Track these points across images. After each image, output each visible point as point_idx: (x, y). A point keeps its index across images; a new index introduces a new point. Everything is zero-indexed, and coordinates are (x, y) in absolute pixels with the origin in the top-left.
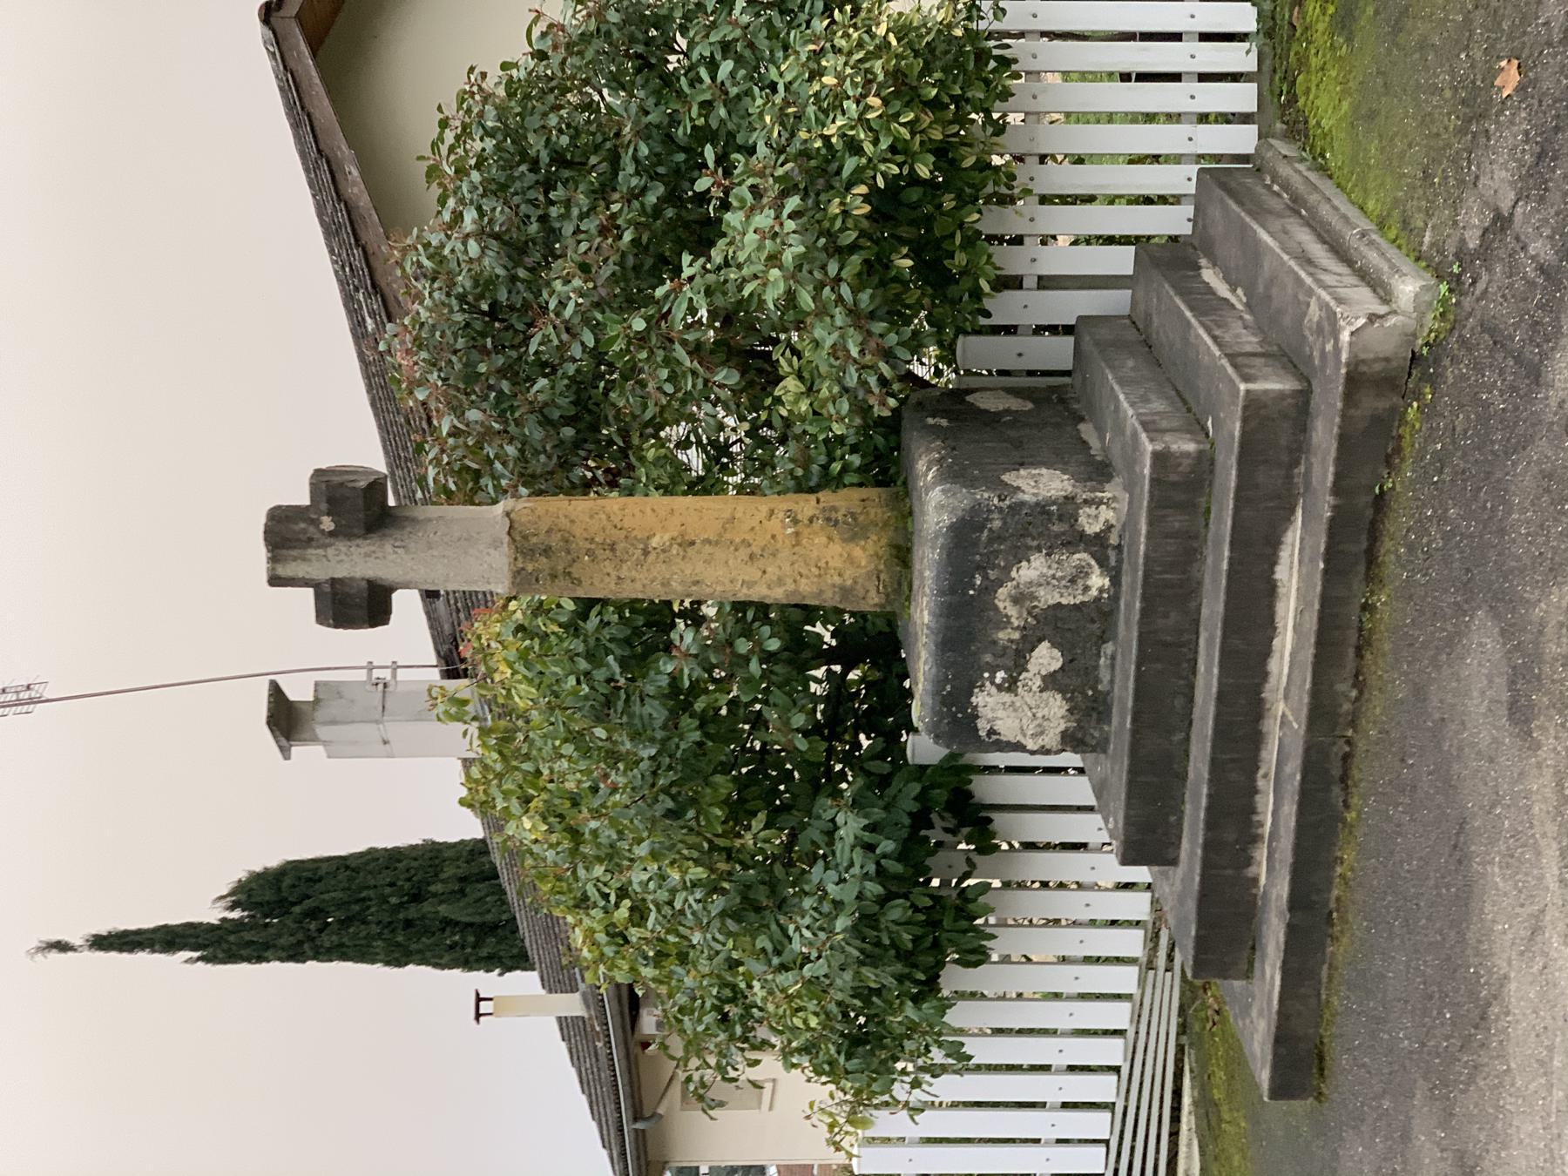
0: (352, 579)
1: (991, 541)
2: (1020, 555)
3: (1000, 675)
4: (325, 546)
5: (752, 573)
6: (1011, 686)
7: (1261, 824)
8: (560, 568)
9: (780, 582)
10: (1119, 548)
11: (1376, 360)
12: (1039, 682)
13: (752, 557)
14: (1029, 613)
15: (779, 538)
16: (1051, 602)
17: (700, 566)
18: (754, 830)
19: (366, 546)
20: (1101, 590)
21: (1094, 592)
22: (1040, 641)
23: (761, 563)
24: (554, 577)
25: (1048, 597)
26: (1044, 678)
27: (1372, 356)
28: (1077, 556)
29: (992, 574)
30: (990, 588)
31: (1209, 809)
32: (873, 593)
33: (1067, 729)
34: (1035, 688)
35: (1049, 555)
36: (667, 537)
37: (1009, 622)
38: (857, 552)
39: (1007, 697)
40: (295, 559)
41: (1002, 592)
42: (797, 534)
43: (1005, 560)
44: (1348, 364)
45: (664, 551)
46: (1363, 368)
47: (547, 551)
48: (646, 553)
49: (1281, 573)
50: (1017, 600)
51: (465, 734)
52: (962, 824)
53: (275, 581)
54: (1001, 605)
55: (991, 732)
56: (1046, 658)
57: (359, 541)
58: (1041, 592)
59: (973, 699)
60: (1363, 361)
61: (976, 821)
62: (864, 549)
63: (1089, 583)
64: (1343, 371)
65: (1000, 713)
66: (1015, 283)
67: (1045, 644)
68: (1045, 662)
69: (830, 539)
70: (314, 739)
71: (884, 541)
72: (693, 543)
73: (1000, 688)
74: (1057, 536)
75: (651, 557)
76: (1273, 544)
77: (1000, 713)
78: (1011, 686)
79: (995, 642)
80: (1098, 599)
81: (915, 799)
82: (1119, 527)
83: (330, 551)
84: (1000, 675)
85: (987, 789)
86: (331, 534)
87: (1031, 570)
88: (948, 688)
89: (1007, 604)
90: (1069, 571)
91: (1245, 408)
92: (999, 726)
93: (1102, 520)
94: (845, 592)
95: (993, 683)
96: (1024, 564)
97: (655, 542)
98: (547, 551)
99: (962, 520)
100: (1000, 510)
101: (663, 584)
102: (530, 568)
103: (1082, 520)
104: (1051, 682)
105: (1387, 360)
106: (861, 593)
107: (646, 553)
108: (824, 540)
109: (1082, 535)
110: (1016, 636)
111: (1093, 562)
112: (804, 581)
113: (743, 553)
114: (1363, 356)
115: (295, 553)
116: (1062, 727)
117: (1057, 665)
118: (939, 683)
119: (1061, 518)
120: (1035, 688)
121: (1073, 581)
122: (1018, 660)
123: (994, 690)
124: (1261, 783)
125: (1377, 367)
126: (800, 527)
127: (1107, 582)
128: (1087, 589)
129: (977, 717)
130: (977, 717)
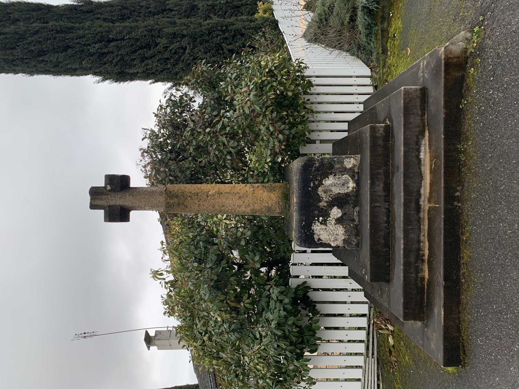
0: (115, 206)
1: (315, 171)
2: (326, 176)
3: (321, 218)
4: (107, 195)
5: (240, 202)
6: (324, 223)
7: (424, 255)
9: (249, 206)
10: (358, 173)
11: (454, 57)
12: (334, 221)
13: (240, 197)
14: (329, 197)
16: (337, 192)
17: (224, 200)
18: (243, 300)
19: (120, 195)
20: (353, 188)
21: (351, 189)
22: (334, 206)
23: (243, 199)
24: (179, 204)
25: (336, 190)
26: (336, 220)
27: (453, 56)
28: (344, 176)
29: (317, 183)
30: (316, 187)
31: (404, 249)
32: (277, 209)
33: (345, 239)
34: (333, 223)
35: (335, 175)
36: (214, 191)
37: (323, 199)
38: (272, 195)
39: (323, 227)
40: (98, 199)
41: (320, 189)
42: (254, 190)
43: (320, 177)
44: (445, 59)
45: (213, 196)
46: (450, 61)
47: (177, 197)
48: (207, 196)
49: (422, 156)
50: (325, 192)
51: (160, 283)
52: (307, 307)
53: (93, 207)
54: (320, 194)
55: (319, 239)
56: (336, 212)
57: (119, 193)
58: (333, 189)
59: (312, 227)
60: (450, 58)
61: (311, 305)
62: (274, 194)
63: (349, 185)
64: (443, 62)
65: (322, 232)
66: (314, 142)
67: (336, 207)
68: (335, 214)
69: (264, 191)
70: (155, 345)
71: (280, 192)
72: (222, 193)
73: (321, 223)
74: (337, 169)
75: (209, 198)
76: (418, 144)
77: (322, 232)
78: (324, 223)
79: (319, 207)
80: (353, 191)
81: (294, 293)
82: (358, 165)
83: (109, 197)
84: (321, 218)
85: (315, 296)
86: (110, 191)
87: (329, 181)
88: (304, 223)
89: (322, 193)
91: (404, 94)
92: (322, 237)
93: (352, 163)
94: (269, 209)
95: (319, 222)
96: (327, 179)
97: (210, 193)
98: (177, 197)
99: (305, 164)
100: (318, 161)
101: (213, 207)
102: (172, 202)
103: (345, 163)
104: (339, 221)
105: (458, 57)
106: (274, 209)
107: (207, 196)
108: (262, 192)
109: (346, 168)
110: (325, 204)
111: (350, 178)
112: (256, 205)
113: (237, 196)
114: (450, 56)
115: (98, 197)
116: (343, 238)
117: (340, 215)
118: (300, 221)
119: (338, 163)
120: (333, 223)
121: (343, 185)
122: (326, 214)
123: (319, 224)
124: (422, 238)
125: (455, 60)
126: (254, 189)
127: (355, 185)
128: (348, 187)
129: (314, 234)
130: (314, 234)
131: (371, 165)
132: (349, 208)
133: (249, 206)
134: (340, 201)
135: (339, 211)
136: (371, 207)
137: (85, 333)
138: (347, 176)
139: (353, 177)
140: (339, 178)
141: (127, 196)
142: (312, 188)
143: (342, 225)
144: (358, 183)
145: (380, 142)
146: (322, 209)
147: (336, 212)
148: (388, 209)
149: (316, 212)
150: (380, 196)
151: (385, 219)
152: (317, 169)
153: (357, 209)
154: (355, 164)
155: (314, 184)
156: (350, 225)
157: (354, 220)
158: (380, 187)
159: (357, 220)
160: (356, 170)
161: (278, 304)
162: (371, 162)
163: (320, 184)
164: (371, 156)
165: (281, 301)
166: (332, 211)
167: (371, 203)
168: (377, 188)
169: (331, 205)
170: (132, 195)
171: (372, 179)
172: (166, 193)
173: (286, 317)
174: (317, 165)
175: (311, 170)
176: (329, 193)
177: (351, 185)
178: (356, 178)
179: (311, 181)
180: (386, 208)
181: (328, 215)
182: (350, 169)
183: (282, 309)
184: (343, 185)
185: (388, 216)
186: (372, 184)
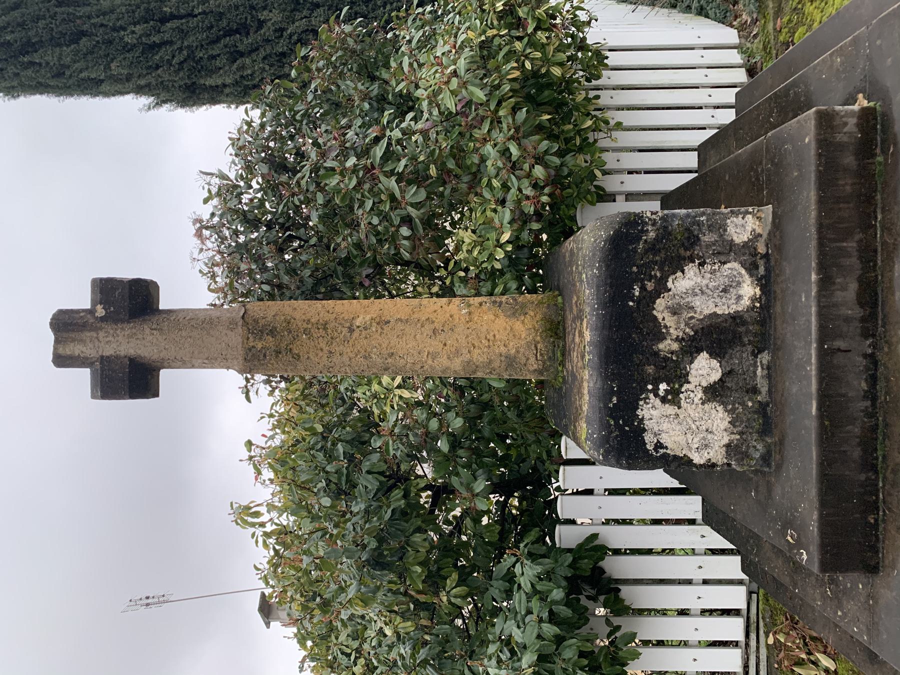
0: (117, 357)
1: (646, 251)
2: (677, 265)
3: (663, 387)
4: (97, 329)
5: (435, 345)
6: (673, 398)
8: (283, 345)
9: (457, 352)
10: (766, 256)
12: (700, 394)
13: (434, 331)
14: (687, 324)
15: (456, 317)
16: (707, 312)
18: (447, 589)
19: (128, 329)
20: (753, 299)
21: (746, 302)
22: (699, 351)
24: (278, 352)
25: (705, 307)
26: (706, 390)
28: (728, 265)
29: (650, 286)
30: (649, 299)
32: (532, 360)
33: (731, 441)
34: (696, 400)
35: (702, 264)
36: (368, 317)
37: (668, 333)
38: (518, 326)
39: (670, 409)
40: (73, 340)
41: (660, 303)
42: (470, 313)
43: (661, 269)
45: (365, 329)
47: (273, 332)
48: (351, 330)
51: (253, 535)
52: (599, 593)
53: (61, 360)
54: (660, 317)
55: (659, 446)
56: (705, 369)
57: (125, 325)
58: (697, 302)
59: (639, 412)
61: (609, 590)
62: (523, 322)
63: (741, 292)
67: (704, 355)
68: (704, 372)
69: (496, 316)
70: (278, 619)
71: (539, 317)
72: (389, 322)
73: (664, 400)
74: (708, 246)
75: (356, 334)
77: (665, 426)
78: (673, 398)
79: (656, 354)
80: (752, 308)
81: (569, 566)
82: (765, 236)
83: (101, 334)
84: (663, 387)
85: (618, 567)
86: (102, 319)
87: (686, 281)
88: (615, 400)
89: (666, 315)
90: (721, 281)
92: (665, 439)
93: (749, 229)
94: (511, 361)
95: (656, 395)
96: (679, 274)
97: (358, 322)
98: (273, 332)
99: (618, 233)
100: (654, 223)
101: (365, 357)
102: (259, 346)
103: (731, 229)
104: (714, 392)
106: (523, 361)
107: (351, 330)
108: (492, 317)
109: (731, 243)
110: (675, 346)
111: (743, 272)
112: (477, 351)
113: (428, 329)
115: (73, 335)
116: (726, 440)
117: (716, 376)
118: (605, 395)
119: (711, 228)
120: (696, 400)
121: (725, 291)
122: (675, 374)
123: (658, 402)
126: (472, 309)
127: (758, 291)
128: (739, 298)
129: (644, 430)
130: (644, 430)
131: (820, 228)
132: (741, 357)
133: (457, 352)
134: (715, 336)
135: (715, 363)
136: (823, 355)
137: (147, 598)
138: (735, 265)
139: (751, 268)
140: (713, 272)
141: (147, 331)
142: (639, 301)
143: (722, 403)
144: (765, 284)
145: (849, 160)
146: (666, 359)
147: (705, 369)
148: (872, 356)
149: (650, 369)
150: (847, 320)
151: (864, 385)
152: (652, 248)
153: (765, 357)
154: (759, 230)
155: (643, 288)
156: (743, 404)
157: (755, 391)
158: (848, 292)
159: (764, 390)
160: (762, 249)
161: (535, 604)
162: (819, 217)
163: (662, 288)
164: (821, 201)
165: (544, 597)
166: (695, 365)
167: (821, 341)
168: (839, 296)
169: (692, 347)
170: (161, 330)
171: (822, 268)
172: (245, 323)
173: (559, 640)
174: (652, 235)
175: (635, 251)
176: (686, 315)
177: (749, 290)
178: (762, 270)
179: (635, 281)
180: (865, 356)
181: (684, 378)
182: (745, 245)
183: (545, 615)
184: (725, 291)
185: (873, 380)
186: (825, 283)
